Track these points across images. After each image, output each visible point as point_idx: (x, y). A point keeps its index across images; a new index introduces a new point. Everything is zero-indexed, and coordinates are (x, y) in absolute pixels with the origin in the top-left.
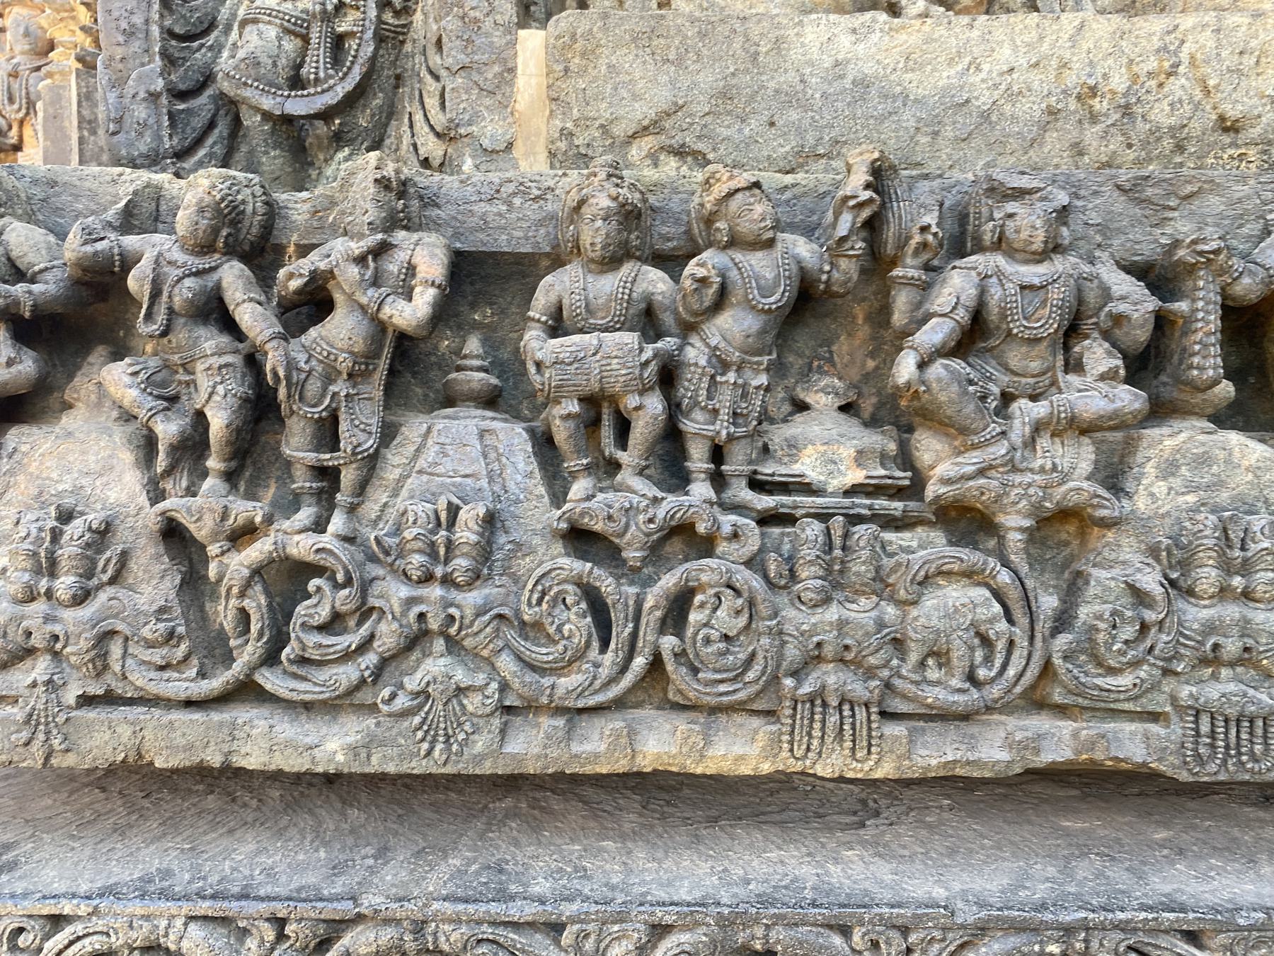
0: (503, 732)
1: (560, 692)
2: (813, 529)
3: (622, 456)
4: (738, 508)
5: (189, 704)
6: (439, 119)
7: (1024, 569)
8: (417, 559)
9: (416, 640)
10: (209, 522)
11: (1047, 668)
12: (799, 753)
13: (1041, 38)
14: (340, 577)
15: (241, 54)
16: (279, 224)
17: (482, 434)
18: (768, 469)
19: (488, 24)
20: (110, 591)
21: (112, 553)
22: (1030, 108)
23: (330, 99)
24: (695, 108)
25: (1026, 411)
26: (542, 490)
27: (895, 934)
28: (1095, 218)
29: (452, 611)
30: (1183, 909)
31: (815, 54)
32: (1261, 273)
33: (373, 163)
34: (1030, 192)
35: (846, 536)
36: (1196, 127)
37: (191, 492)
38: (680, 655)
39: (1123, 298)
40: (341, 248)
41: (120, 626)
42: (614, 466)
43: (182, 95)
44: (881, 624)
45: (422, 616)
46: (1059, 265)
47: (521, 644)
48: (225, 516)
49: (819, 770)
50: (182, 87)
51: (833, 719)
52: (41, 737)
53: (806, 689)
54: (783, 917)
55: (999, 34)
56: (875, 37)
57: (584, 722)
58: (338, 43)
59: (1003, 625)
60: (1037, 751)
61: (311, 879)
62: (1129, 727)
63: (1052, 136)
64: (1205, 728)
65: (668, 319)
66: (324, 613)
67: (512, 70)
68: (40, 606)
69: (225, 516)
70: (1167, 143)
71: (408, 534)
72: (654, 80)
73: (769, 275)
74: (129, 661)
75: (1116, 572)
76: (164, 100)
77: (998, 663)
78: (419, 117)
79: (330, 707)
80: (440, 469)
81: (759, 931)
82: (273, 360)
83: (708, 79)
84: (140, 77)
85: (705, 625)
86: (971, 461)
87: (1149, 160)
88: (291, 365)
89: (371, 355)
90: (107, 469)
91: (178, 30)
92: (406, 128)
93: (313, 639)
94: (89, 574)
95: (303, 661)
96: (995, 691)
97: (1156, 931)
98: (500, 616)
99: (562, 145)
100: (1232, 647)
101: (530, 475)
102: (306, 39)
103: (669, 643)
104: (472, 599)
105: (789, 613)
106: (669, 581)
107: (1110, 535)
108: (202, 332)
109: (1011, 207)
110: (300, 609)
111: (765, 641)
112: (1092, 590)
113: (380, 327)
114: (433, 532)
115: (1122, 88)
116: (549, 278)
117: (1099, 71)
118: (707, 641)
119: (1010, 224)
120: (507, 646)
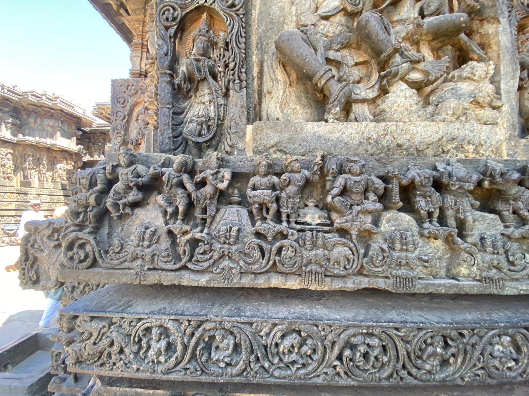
0: (240, 278)
1: (253, 269)
2: (309, 233)
3: (268, 216)
4: (293, 228)
5: (171, 270)
6: (230, 143)
8: (223, 239)
9: (222, 257)
10: (178, 230)
11: (362, 266)
12: (306, 284)
13: (358, 127)
14: (206, 243)
15: (188, 129)
16: (196, 166)
17: (237, 211)
18: (299, 219)
19: (241, 124)
20: (155, 245)
21: (156, 237)
22: (356, 142)
23: (207, 139)
24: (284, 142)
25: (356, 208)
26: (250, 224)
27: (328, 327)
28: (370, 166)
29: (230, 250)
30: (394, 322)
31: (309, 130)
32: (408, 179)
33: (216, 154)
34: (356, 161)
35: (317, 235)
37: (174, 223)
38: (280, 261)
39: (377, 184)
40: (209, 172)
41: (157, 253)
42: (266, 219)
43: (176, 137)
44: (324, 255)
45: (223, 252)
46: (363, 177)
47: (245, 258)
48: (181, 229)
49: (311, 288)
50: (176, 135)
51: (314, 276)
52: (139, 277)
53: (308, 269)
54: (302, 322)
55: (349, 126)
56: (322, 127)
57: (258, 276)
58: (209, 127)
59: (352, 256)
60: (360, 285)
61: (197, 310)
62: (381, 280)
63: (361, 148)
64: (398, 280)
65: (278, 187)
66: (202, 250)
67: (245, 133)
68: (140, 248)
69: (181, 229)
70: (386, 149)
71: (221, 233)
72: (275, 136)
73: (299, 178)
74: (159, 261)
75: (377, 244)
77: (351, 264)
78: (226, 142)
79: (202, 272)
80: (228, 219)
81: (297, 326)
82: (193, 195)
83: (286, 136)
84: (167, 134)
85: (286, 254)
86: (344, 219)
87: (382, 153)
88: (197, 197)
89: (214, 194)
90: (156, 218)
91: (175, 124)
92: (223, 145)
93: (199, 256)
94: (151, 241)
95: (197, 261)
96: (351, 271)
98: (240, 252)
99: (256, 149)
100: (404, 262)
101: (247, 220)
102: (202, 126)
103: (277, 258)
104: (234, 248)
105: (304, 252)
106: (278, 244)
107: (376, 236)
108: (178, 189)
109: (352, 164)
110: (197, 250)
111: (299, 258)
112: (372, 248)
113: (216, 189)
114: (226, 233)
115: (376, 138)
116: (252, 178)
117: (371, 134)
118: (286, 258)
119: (352, 168)
120: (242, 258)
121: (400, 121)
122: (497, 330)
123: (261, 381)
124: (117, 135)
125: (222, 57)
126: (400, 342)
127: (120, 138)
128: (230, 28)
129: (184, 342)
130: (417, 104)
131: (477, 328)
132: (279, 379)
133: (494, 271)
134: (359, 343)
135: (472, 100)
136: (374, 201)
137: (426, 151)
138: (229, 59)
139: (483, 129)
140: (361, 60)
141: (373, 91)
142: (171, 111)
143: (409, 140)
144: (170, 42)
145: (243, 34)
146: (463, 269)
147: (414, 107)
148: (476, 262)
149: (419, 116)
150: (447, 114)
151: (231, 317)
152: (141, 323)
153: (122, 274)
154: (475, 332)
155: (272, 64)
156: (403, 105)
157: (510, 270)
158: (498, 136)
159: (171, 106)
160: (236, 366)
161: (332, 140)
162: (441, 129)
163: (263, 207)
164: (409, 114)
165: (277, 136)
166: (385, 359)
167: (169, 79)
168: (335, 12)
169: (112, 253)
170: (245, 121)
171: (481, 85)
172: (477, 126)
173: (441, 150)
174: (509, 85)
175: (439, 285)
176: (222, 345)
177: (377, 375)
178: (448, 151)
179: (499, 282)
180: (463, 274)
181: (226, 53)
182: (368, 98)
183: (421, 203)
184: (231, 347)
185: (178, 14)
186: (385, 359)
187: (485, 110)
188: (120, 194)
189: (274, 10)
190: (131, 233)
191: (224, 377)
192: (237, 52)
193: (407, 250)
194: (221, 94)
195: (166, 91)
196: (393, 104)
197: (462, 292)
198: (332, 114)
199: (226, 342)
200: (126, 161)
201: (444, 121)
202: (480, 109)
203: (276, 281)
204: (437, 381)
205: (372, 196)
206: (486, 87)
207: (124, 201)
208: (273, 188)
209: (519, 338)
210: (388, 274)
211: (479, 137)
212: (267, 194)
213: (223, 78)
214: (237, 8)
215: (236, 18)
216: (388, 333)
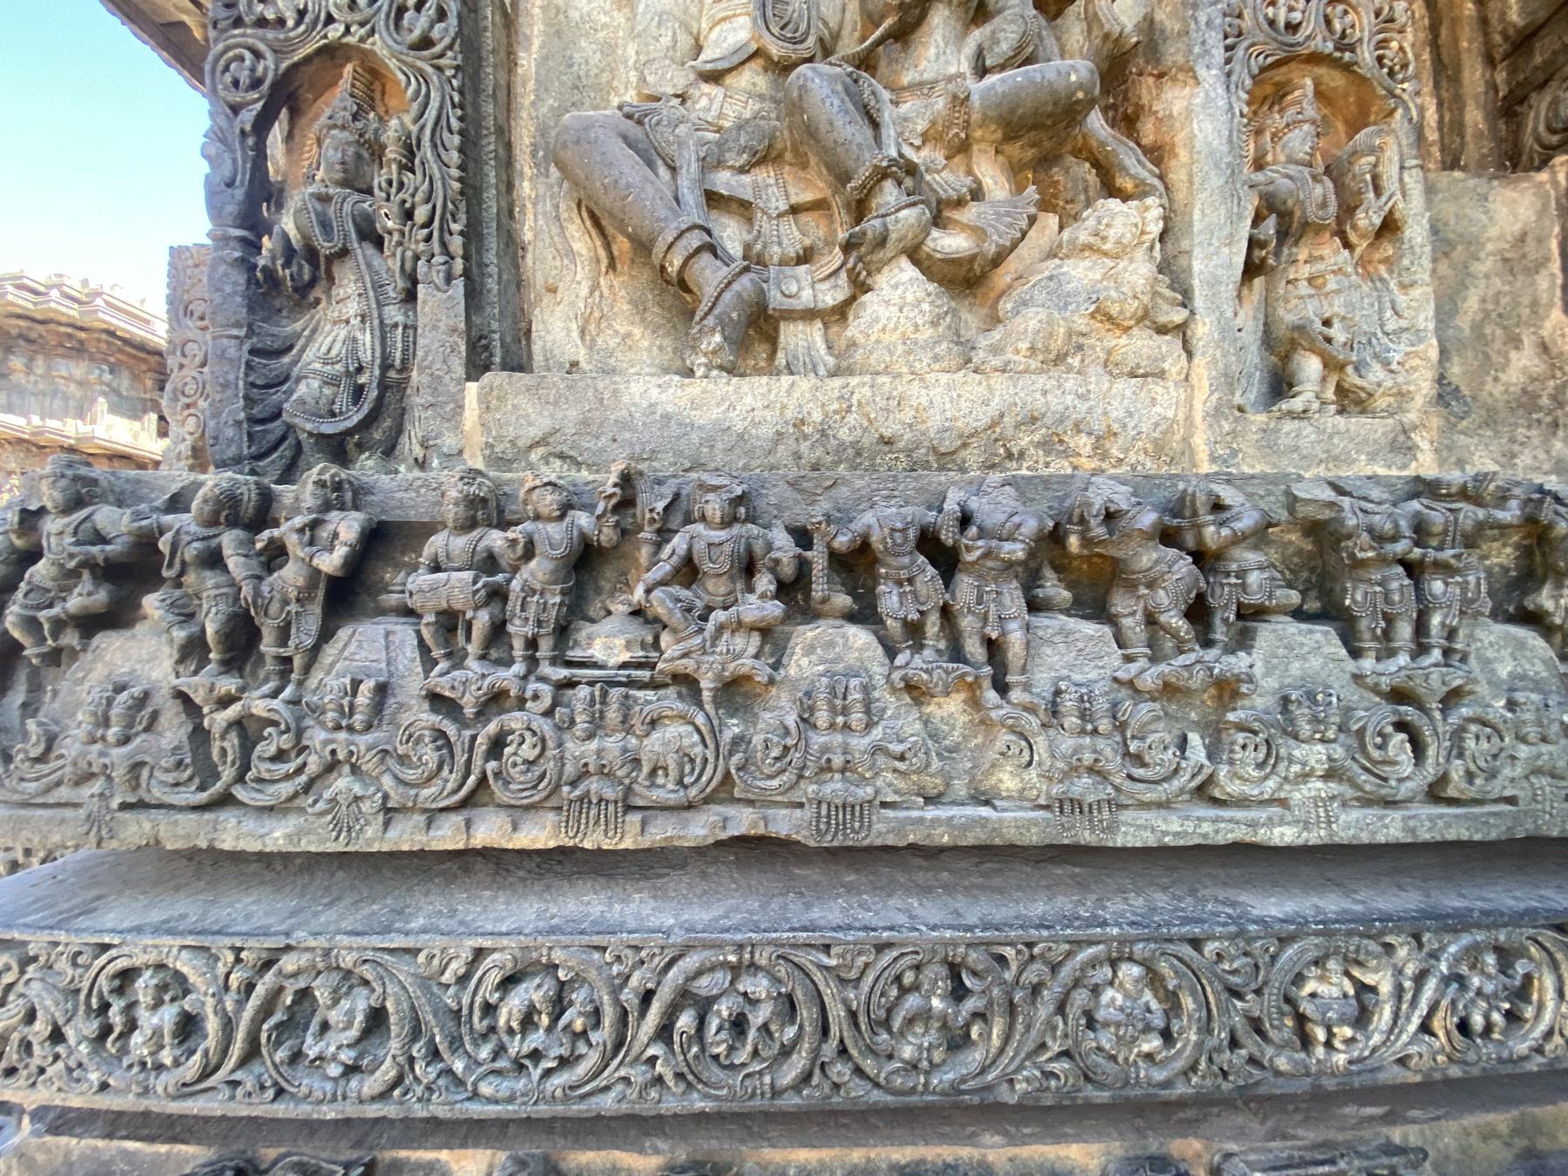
1: (421, 799)
7: (712, 713)
9: (332, 766)
10: (201, 691)
13: (770, 391)
14: (283, 727)
18: (575, 654)
20: (144, 736)
22: (767, 431)
23: (350, 424)
26: (420, 669)
27: (629, 952)
28: (773, 500)
29: (353, 748)
32: (850, 535)
34: (720, 487)
36: (866, 441)
37: (195, 673)
41: (147, 759)
43: (262, 421)
44: (625, 750)
45: (333, 752)
46: (736, 529)
47: (397, 768)
50: (259, 416)
51: (593, 812)
52: (95, 829)
53: (577, 793)
56: (672, 390)
59: (699, 749)
62: (784, 812)
63: (781, 448)
65: (503, 563)
66: (272, 750)
67: (462, 407)
68: (98, 747)
72: (540, 414)
73: (558, 537)
74: (153, 781)
76: (245, 426)
81: (545, 952)
82: (247, 591)
83: (573, 413)
84: (229, 413)
87: (840, 462)
91: (258, 382)
94: (130, 725)
95: (260, 780)
96: (693, 792)
97: (795, 946)
98: (385, 752)
100: (837, 761)
101: (413, 660)
103: (492, 765)
104: (363, 741)
110: (259, 748)
115: (819, 420)
117: (805, 410)
120: (388, 769)
121: (886, 371)
122: (1101, 947)
123: (442, 1112)
124: (186, 413)
125: (393, 190)
126: (828, 985)
127: (192, 420)
128: (415, 106)
129: (224, 1009)
132: (497, 1102)
133: (1086, 780)
134: (715, 992)
135: (1093, 308)
136: (763, 596)
137: (963, 453)
138: (413, 196)
139: (1114, 391)
140: (807, 197)
141: (836, 286)
142: (246, 347)
143: (911, 425)
144: (243, 149)
145: (455, 124)
146: (1005, 777)
147: (927, 333)
148: (1036, 758)
149: (936, 358)
150: (1017, 352)
151: (358, 934)
152: (104, 959)
153: (49, 821)
154: (1036, 951)
155: (557, 207)
156: (896, 329)
157: (1130, 777)
158: (1158, 409)
159: (242, 332)
160: (372, 1072)
163: (450, 622)
164: (910, 352)
165: (546, 413)
166: (791, 1032)
167: (237, 254)
168: (736, 60)
169: (22, 761)
170: (460, 371)
171: (1122, 265)
172: (1097, 380)
173: (1002, 451)
175: (936, 821)
176: (335, 1016)
177: (767, 1079)
178: (1022, 454)
179: (1100, 812)
180: (1008, 790)
181: (408, 177)
182: (821, 305)
183: (890, 600)
184: (360, 1018)
185: (266, 69)
186: (791, 1032)
187: (1130, 337)
188: (49, 591)
189: (583, 50)
190: (79, 704)
191: (339, 1106)
192: (437, 175)
194: (393, 295)
195: (228, 289)
196: (870, 326)
197: (997, 841)
198: (705, 354)
199: (345, 1004)
200: (57, 495)
201: (1004, 371)
202: (1118, 332)
203: (489, 831)
204: (934, 1092)
205: (764, 582)
206: (1134, 272)
207: (56, 610)
208: (490, 563)
210: (796, 796)
212: (459, 586)
213: (399, 250)
214: (437, 49)
215: (435, 78)
216: (796, 960)
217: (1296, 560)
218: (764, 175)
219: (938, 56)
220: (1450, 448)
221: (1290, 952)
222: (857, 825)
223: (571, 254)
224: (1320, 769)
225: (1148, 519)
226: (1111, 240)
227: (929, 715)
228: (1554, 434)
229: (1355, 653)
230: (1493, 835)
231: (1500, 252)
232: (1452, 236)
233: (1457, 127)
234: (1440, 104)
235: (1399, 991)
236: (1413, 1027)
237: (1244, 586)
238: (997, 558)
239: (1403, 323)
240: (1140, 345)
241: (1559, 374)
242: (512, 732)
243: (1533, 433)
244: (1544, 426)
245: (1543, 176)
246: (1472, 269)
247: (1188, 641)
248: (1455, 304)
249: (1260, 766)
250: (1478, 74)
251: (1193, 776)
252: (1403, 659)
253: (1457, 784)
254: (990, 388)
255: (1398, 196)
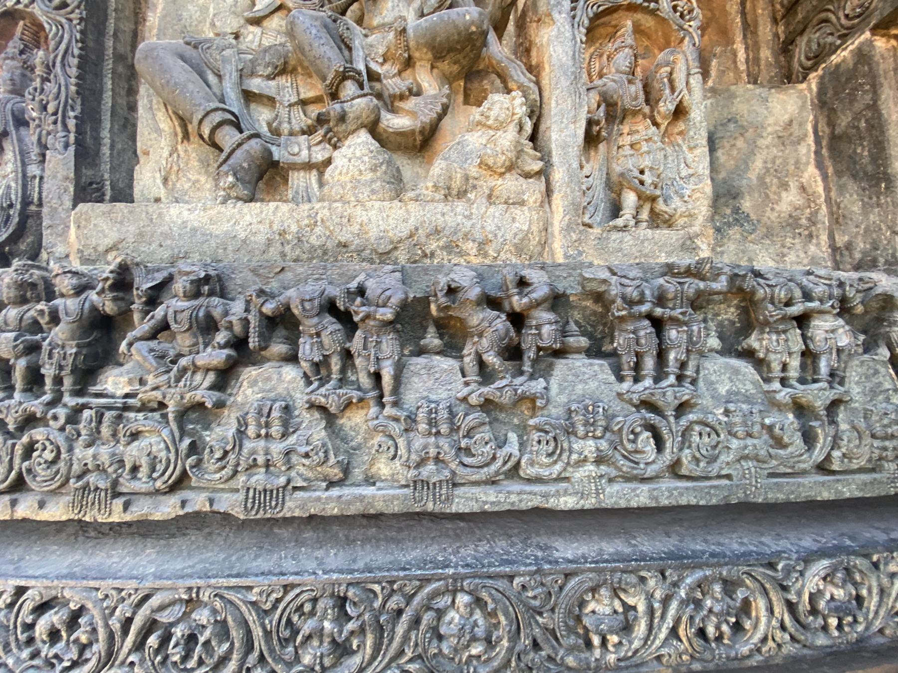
13: (261, 212)
22: (261, 238)
24: (129, 240)
25: (183, 362)
27: (114, 593)
28: (239, 282)
36: (329, 245)
44: (114, 454)
56: (197, 212)
59: (163, 455)
63: (272, 249)
73: (72, 308)
115: (295, 231)
117: (286, 225)
122: (442, 582)
126: (251, 614)
130: (374, 169)
131: (398, 579)
134: (171, 620)
135: (479, 161)
137: (396, 253)
139: (488, 213)
141: (324, 149)
146: (382, 466)
147: (369, 176)
148: (399, 453)
149: (373, 192)
150: (427, 188)
154: (395, 587)
156: (347, 173)
158: (517, 225)
161: (216, 236)
162: (413, 214)
164: (355, 188)
165: (115, 229)
166: (226, 646)
168: (267, 12)
172: (479, 206)
173: (420, 252)
174: (566, 132)
179: (441, 489)
182: (314, 160)
186: (226, 646)
187: (504, 179)
189: (189, 10)
193: (268, 436)
198: (224, 189)
201: (417, 200)
202: (496, 177)
209: (484, 595)
211: (483, 228)
213: (38, 130)
217: (593, 318)
218: (283, 81)
219: (393, 8)
220: (743, 252)
221: (572, 582)
222: (274, 503)
223: (159, 131)
224: (592, 457)
225: (474, 293)
226: (492, 118)
227: (342, 425)
228: (810, 241)
229: (621, 379)
230: (714, 501)
231: (776, 131)
232: (745, 124)
233: (757, 60)
234: (747, 49)
235: (651, 612)
236: (662, 635)
237: (539, 334)
238: (375, 319)
239: (691, 171)
240: (511, 184)
241: (812, 205)
242: (37, 442)
243: (797, 241)
244: (803, 237)
245: (803, 86)
246: (758, 143)
247: (501, 372)
248: (748, 165)
249: (550, 455)
250: (768, 29)
251: (505, 463)
252: (648, 382)
253: (687, 467)
254: (407, 211)
255: (685, 91)
